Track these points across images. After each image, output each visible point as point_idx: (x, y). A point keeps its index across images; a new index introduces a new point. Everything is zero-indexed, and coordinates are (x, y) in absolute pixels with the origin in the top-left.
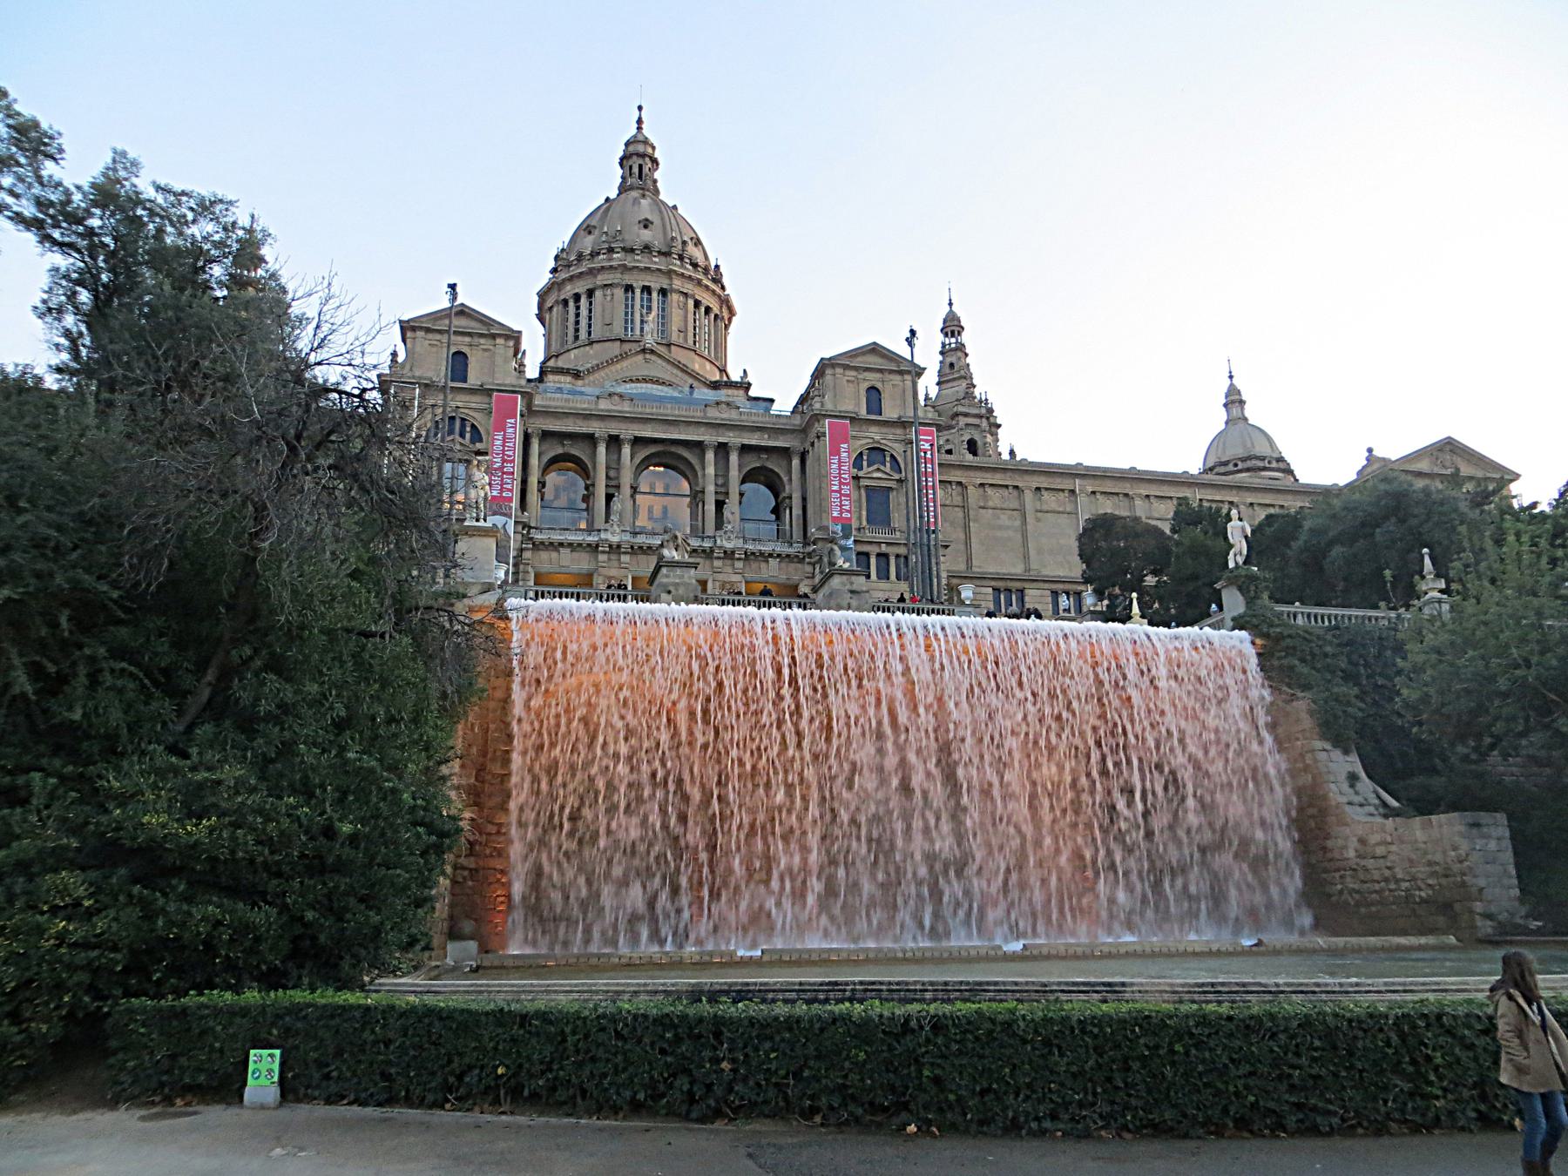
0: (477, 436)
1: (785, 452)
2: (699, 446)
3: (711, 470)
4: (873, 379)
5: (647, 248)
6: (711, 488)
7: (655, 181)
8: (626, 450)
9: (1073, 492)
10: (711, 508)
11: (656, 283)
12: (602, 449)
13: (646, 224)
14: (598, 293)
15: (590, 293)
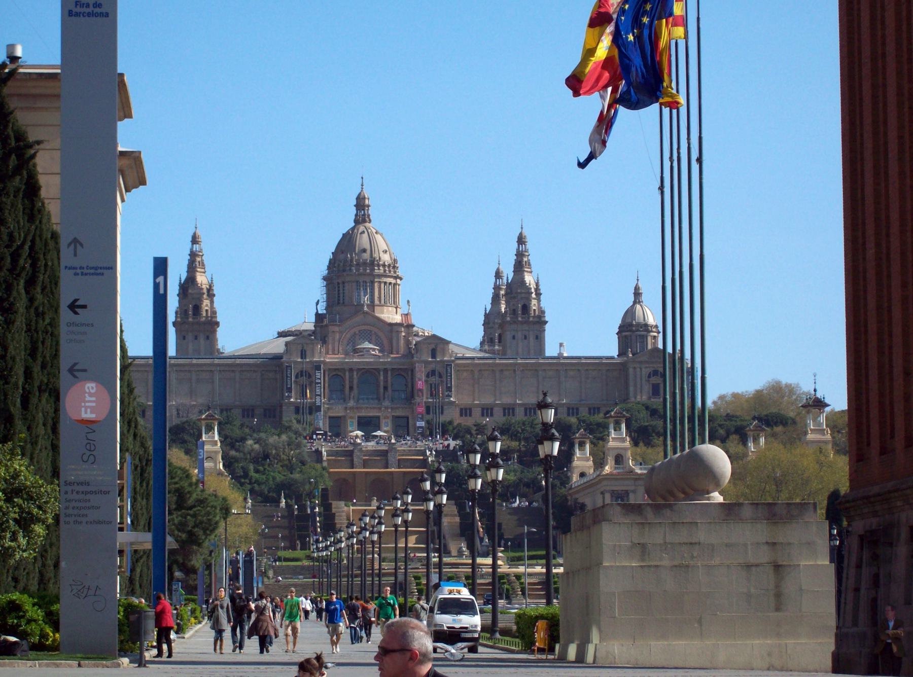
0: (310, 376)
1: (405, 370)
2: (378, 370)
3: (382, 378)
4: (433, 346)
5: (365, 263)
6: (382, 384)
7: (369, 216)
8: (355, 373)
9: (515, 371)
10: (382, 390)
11: (368, 279)
12: (347, 373)
13: (364, 251)
14: (346, 285)
15: (343, 283)
